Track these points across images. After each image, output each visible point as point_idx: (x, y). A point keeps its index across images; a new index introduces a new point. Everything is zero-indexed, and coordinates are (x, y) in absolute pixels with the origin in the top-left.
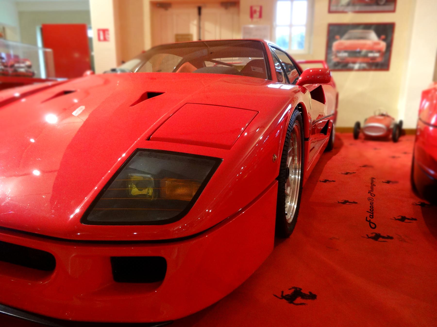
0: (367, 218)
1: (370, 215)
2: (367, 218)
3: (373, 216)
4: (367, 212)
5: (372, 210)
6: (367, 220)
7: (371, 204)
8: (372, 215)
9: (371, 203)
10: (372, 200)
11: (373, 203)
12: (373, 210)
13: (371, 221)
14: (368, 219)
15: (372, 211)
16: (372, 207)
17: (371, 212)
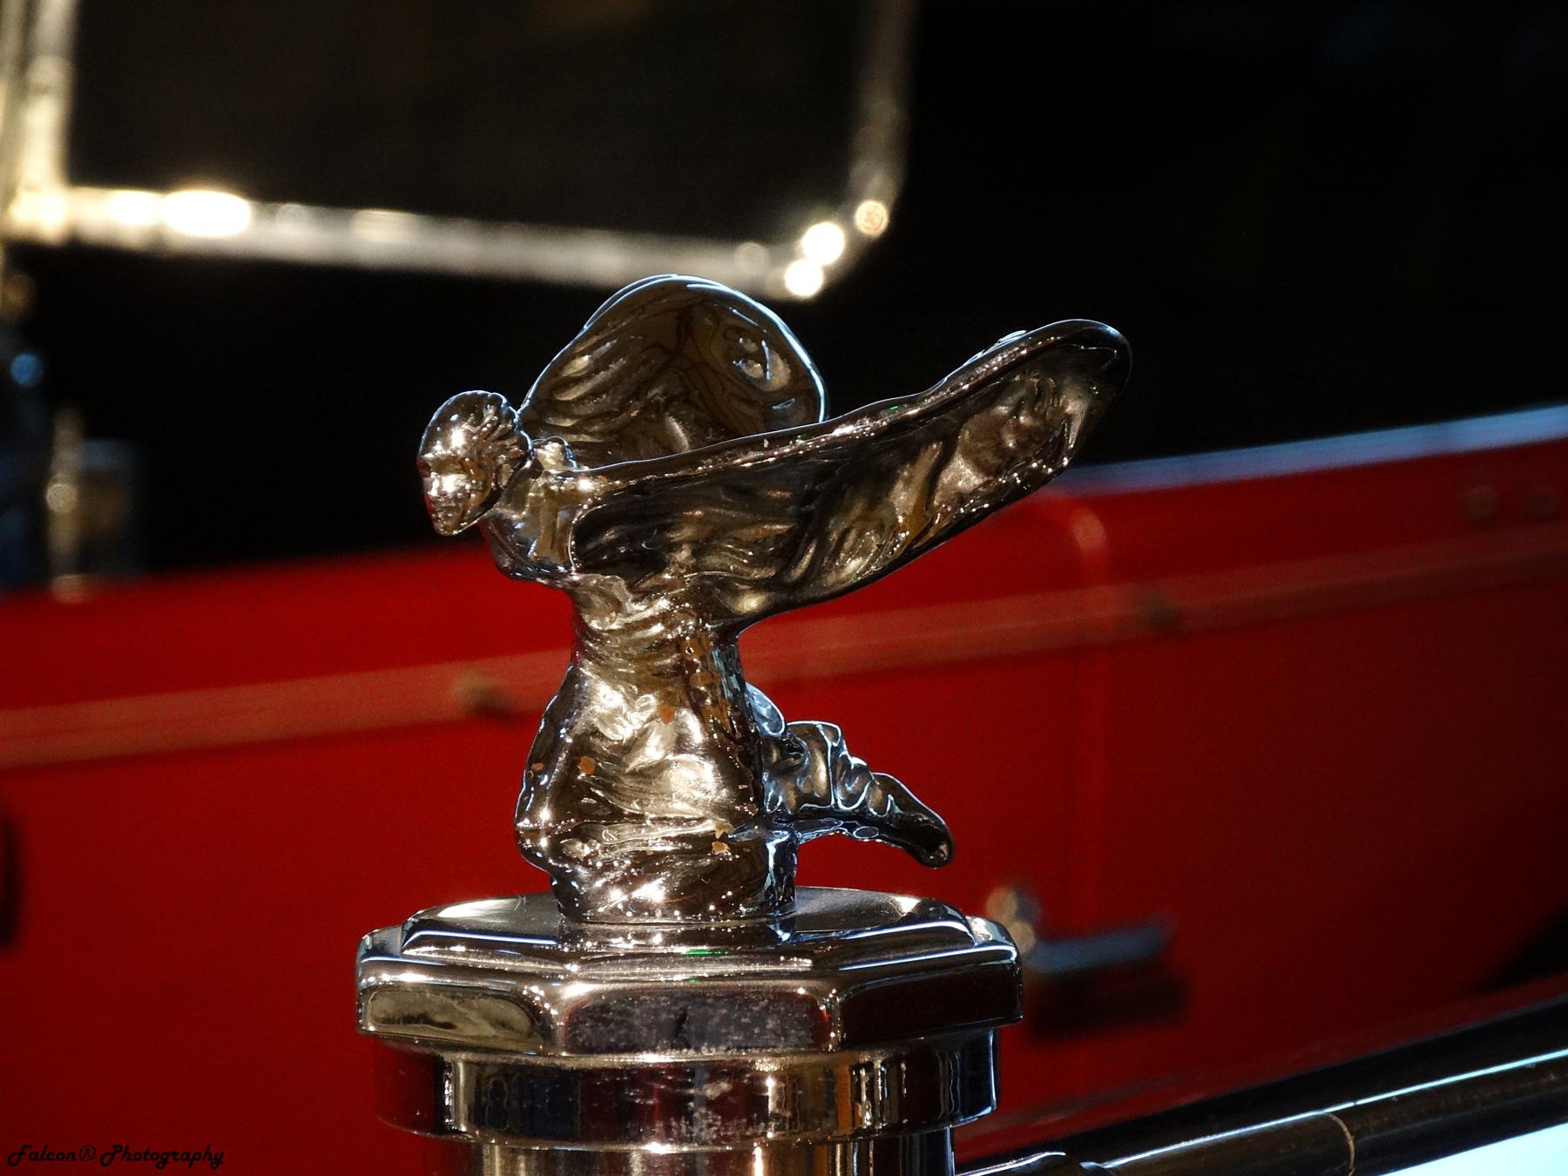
0: (30, 1146)
1: (37, 1154)
2: (30, 1146)
3: (36, 1159)
4: (46, 1147)
5: (51, 1157)
6: (25, 1147)
7: (69, 1154)
8: (39, 1157)
9: (74, 1154)
10: (87, 1158)
11: (73, 1159)
12: (52, 1160)
13: (23, 1156)
14: (26, 1149)
15: (49, 1154)
16: (60, 1157)
17: (47, 1153)
